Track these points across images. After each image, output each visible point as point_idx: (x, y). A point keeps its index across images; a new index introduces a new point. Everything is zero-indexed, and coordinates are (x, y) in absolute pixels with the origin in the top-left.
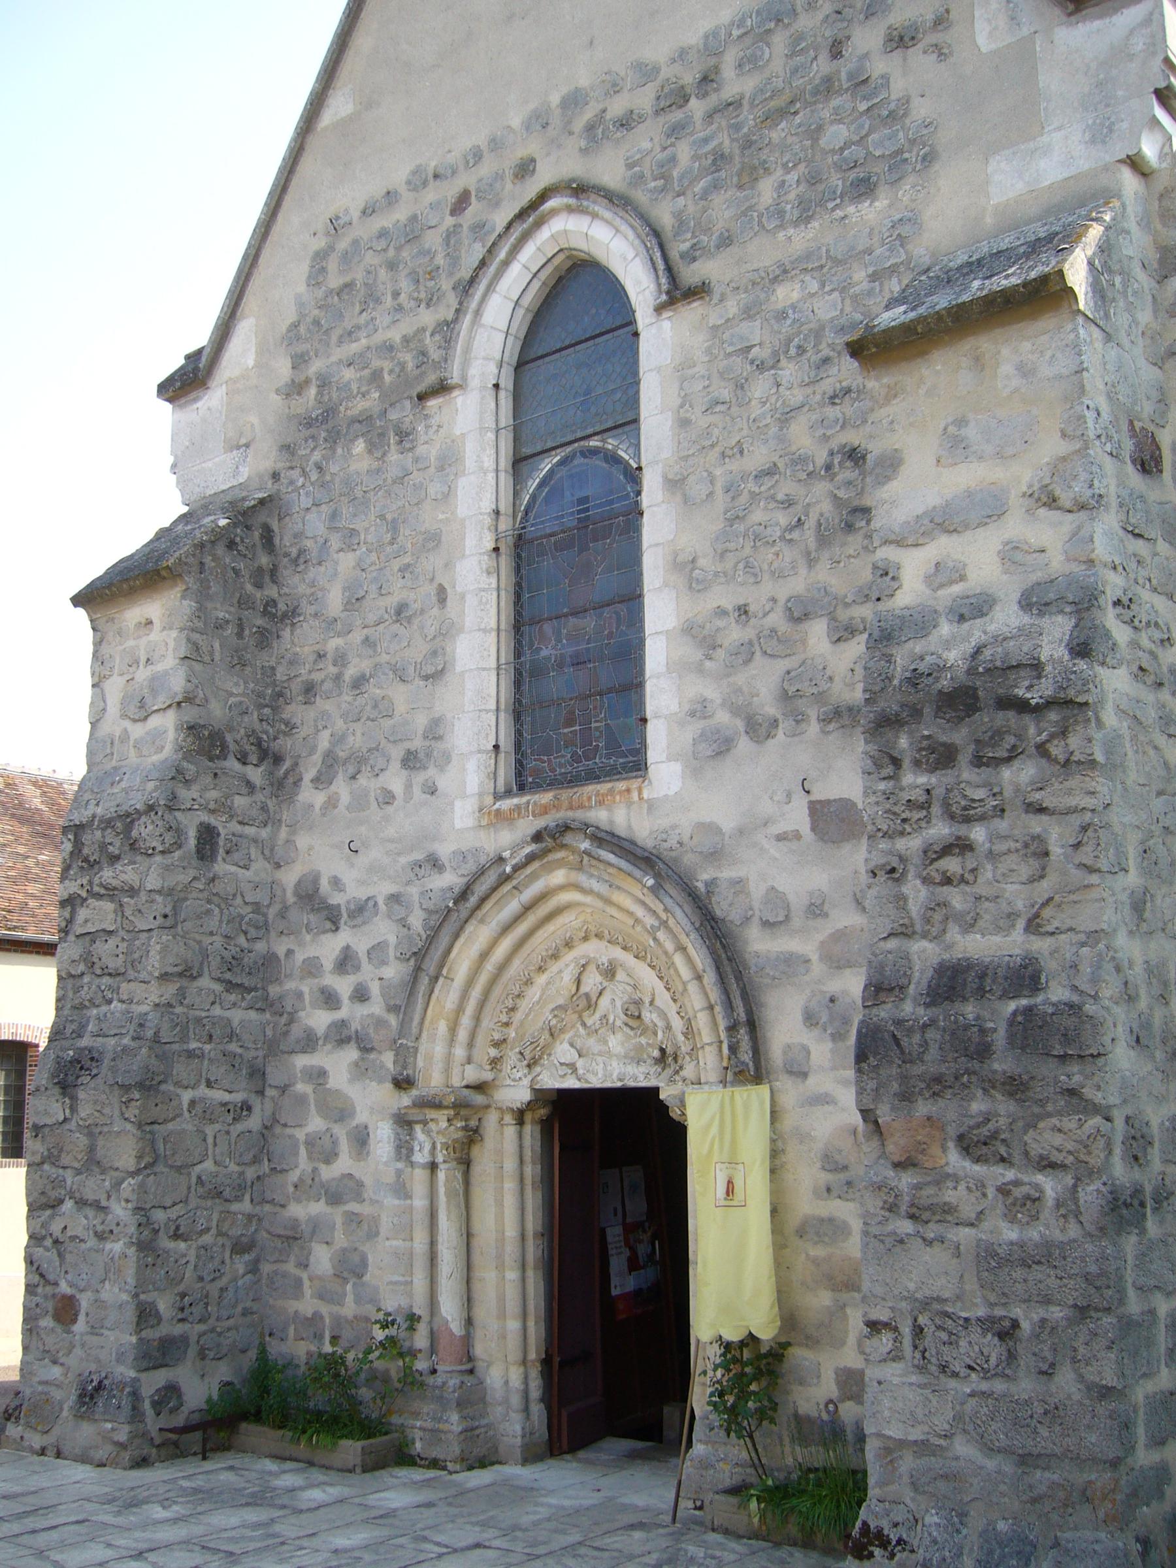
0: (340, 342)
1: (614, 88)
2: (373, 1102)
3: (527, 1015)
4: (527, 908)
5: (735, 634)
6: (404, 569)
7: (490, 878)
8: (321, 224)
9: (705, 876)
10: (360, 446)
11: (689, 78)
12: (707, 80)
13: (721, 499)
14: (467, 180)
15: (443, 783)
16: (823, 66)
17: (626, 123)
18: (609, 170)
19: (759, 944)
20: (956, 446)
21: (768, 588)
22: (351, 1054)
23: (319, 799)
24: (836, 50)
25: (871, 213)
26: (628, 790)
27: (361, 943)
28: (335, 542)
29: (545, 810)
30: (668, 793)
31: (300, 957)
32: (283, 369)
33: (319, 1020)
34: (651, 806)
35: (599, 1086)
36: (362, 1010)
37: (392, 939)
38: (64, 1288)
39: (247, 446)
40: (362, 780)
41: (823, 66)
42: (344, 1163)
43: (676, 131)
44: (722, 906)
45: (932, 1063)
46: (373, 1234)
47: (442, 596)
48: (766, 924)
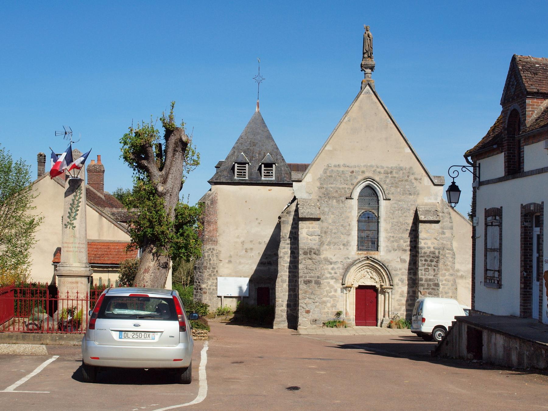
1: (377, 167)
2: (339, 286)
5: (392, 239)
6: (343, 220)
7: (358, 261)
8: (326, 165)
10: (335, 201)
11: (389, 171)
12: (391, 172)
14: (354, 169)
15: (349, 249)
16: (406, 178)
17: (380, 172)
18: (377, 178)
19: (393, 273)
20: (427, 232)
21: (396, 235)
22: (334, 280)
23: (328, 247)
24: (408, 176)
27: (336, 267)
28: (330, 213)
30: (381, 255)
31: (324, 267)
32: (318, 184)
33: (328, 275)
38: (307, 309)
40: (336, 246)
41: (406, 178)
42: (333, 293)
43: (387, 177)
44: (390, 268)
45: (426, 287)
46: (338, 301)
47: (349, 225)
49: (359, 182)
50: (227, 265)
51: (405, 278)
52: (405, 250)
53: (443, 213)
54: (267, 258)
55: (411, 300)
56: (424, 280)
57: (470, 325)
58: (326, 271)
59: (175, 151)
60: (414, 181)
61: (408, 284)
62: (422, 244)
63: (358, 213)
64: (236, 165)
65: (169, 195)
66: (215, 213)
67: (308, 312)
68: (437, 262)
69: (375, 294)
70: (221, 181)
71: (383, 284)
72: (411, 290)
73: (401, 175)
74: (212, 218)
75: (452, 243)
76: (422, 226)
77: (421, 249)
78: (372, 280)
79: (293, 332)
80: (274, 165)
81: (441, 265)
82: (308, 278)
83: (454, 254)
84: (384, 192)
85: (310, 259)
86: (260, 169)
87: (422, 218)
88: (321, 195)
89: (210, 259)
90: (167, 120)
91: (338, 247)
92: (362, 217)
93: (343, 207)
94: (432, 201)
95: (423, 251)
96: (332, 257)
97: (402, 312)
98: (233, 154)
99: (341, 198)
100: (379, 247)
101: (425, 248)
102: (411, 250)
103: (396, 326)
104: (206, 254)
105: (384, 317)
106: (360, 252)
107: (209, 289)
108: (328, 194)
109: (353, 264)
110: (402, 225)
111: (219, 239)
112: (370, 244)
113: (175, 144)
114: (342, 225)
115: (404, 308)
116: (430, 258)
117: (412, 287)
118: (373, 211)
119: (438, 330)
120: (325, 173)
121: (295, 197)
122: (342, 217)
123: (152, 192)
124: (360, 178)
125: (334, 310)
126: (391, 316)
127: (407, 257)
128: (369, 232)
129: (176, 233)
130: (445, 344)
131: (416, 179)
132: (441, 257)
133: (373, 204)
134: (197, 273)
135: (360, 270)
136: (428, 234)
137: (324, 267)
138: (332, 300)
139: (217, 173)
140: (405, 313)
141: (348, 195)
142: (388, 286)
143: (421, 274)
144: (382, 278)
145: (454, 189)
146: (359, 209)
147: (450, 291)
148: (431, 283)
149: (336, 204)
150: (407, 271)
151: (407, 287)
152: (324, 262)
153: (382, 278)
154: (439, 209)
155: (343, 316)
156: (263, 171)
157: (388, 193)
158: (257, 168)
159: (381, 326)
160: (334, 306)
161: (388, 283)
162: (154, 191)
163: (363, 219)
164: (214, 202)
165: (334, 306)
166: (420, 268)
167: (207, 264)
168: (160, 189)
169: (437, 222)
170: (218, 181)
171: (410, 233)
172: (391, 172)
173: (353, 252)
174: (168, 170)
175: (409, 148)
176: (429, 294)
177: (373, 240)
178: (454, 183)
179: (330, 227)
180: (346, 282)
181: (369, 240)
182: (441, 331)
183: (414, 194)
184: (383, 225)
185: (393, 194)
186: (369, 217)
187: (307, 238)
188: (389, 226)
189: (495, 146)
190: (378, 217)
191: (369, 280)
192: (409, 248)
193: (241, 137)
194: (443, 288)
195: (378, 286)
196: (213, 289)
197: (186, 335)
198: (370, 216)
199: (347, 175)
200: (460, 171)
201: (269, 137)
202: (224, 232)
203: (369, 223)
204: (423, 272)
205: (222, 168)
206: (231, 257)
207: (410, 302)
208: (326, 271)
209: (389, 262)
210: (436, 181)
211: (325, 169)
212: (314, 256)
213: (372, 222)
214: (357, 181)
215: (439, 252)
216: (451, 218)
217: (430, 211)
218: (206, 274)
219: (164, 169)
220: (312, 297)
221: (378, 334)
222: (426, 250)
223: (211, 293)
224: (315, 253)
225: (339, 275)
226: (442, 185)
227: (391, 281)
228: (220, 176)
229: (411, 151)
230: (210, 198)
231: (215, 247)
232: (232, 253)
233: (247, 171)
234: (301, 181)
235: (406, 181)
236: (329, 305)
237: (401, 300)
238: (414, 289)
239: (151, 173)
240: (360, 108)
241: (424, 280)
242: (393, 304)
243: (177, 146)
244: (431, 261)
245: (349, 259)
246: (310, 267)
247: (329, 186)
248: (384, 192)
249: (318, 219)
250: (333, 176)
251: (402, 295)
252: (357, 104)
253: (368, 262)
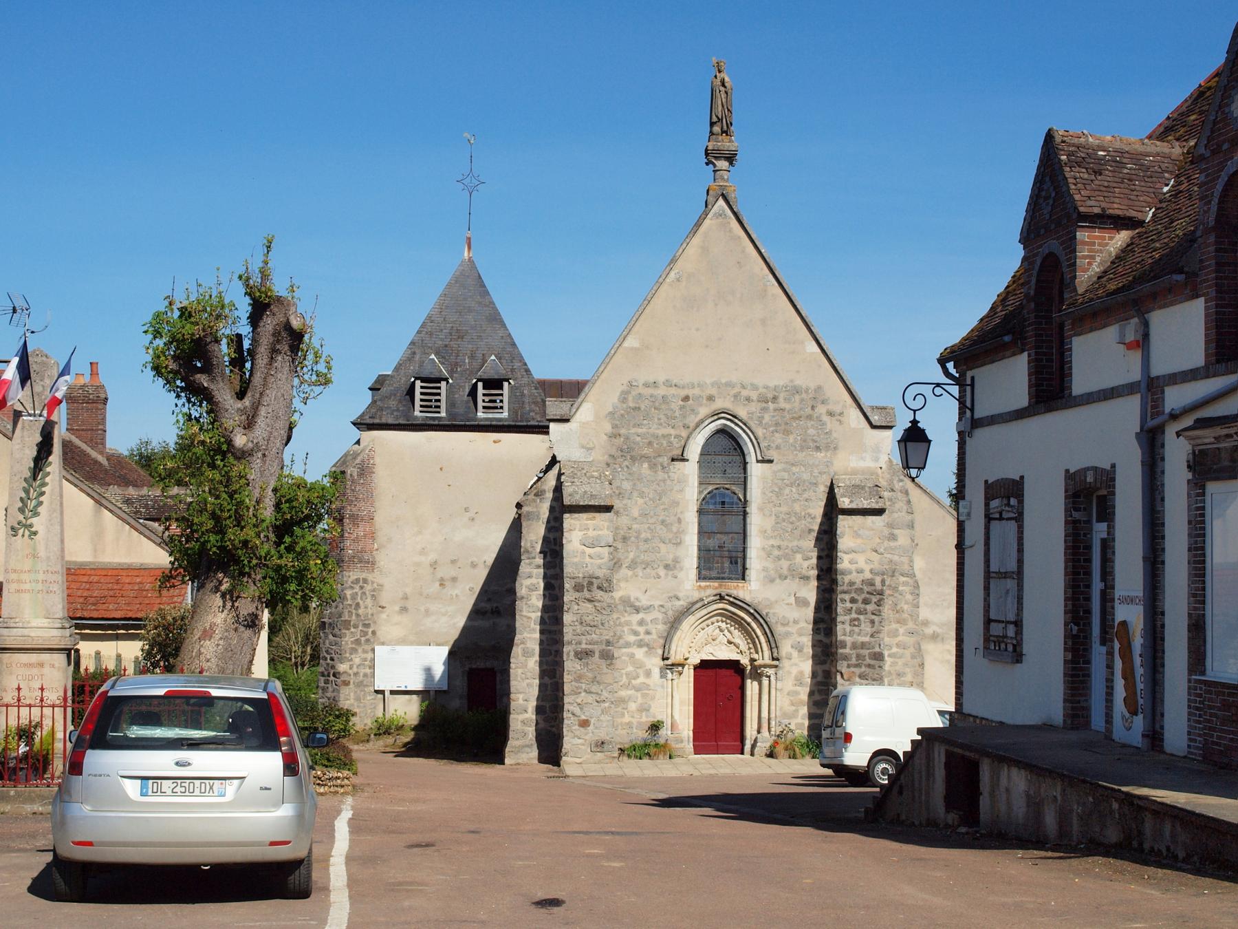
0: (634, 426)
1: (743, 387)
2: (655, 663)
5: (776, 553)
6: (664, 510)
8: (625, 382)
10: (646, 465)
11: (770, 396)
12: (775, 398)
13: (774, 517)
14: (690, 393)
15: (681, 575)
16: (808, 411)
17: (748, 399)
18: (742, 413)
19: (779, 630)
20: (856, 535)
21: (786, 543)
22: (645, 649)
23: (630, 573)
24: (813, 408)
25: (820, 455)
28: (635, 494)
30: (753, 589)
31: (623, 620)
32: (608, 427)
36: (648, 637)
38: (583, 717)
39: (589, 449)
40: (648, 570)
41: (808, 411)
42: (642, 679)
43: (764, 409)
44: (772, 620)
45: (854, 661)
46: (653, 698)
47: (679, 521)
48: (783, 625)
49: (702, 421)
50: (397, 618)
51: (807, 641)
52: (805, 578)
53: (893, 490)
54: (489, 600)
55: (820, 691)
56: (849, 645)
57: (951, 749)
58: (626, 629)
59: (274, 351)
60: (825, 418)
61: (814, 656)
62: (845, 562)
63: (700, 492)
64: (418, 384)
65: (260, 455)
66: (370, 497)
67: (584, 724)
68: (879, 603)
69: (739, 679)
70: (384, 421)
71: (756, 656)
72: (820, 669)
73: (797, 404)
74: (362, 508)
75: (912, 561)
76: (845, 523)
77: (843, 574)
79: (550, 770)
80: (506, 384)
81: (886, 610)
82: (584, 646)
83: (917, 586)
84: (757, 444)
85: (590, 601)
86: (473, 393)
87: (844, 502)
88: (613, 451)
89: (358, 605)
90: (256, 279)
91: (653, 573)
92: (707, 503)
93: (664, 481)
94: (867, 463)
95: (847, 579)
96: (639, 595)
97: (799, 720)
98: (410, 358)
99: (660, 460)
100: (747, 572)
101: (850, 573)
102: (819, 578)
103: (787, 753)
104: (348, 593)
105: (759, 732)
106: (703, 584)
107: (356, 674)
108: (630, 449)
110: (799, 519)
111: (377, 559)
112: (727, 564)
113: (273, 335)
114: (663, 522)
115: (804, 710)
116: (863, 596)
117: (823, 663)
118: (734, 488)
119: (879, 761)
120: (623, 399)
121: (554, 457)
122: (663, 504)
123: (220, 448)
124: (704, 411)
125: (644, 719)
126: (776, 730)
127: (810, 593)
128: (724, 538)
129: (278, 544)
130: (896, 789)
131: (831, 414)
132: (888, 592)
133: (734, 472)
134: (326, 637)
136: (859, 541)
137: (623, 620)
138: (639, 695)
139: (374, 402)
140: (806, 723)
141: (678, 452)
142: (767, 661)
143: (843, 631)
144: (754, 643)
145: (915, 437)
146: (701, 484)
147: (908, 670)
148: (866, 652)
149: (648, 472)
150: (811, 626)
151: (810, 662)
152: (621, 607)
153: (754, 643)
154: (883, 483)
155: (665, 732)
156: (480, 398)
157: (768, 447)
158: (467, 390)
159: (752, 754)
160: (644, 709)
162: (224, 447)
163: (711, 507)
164: (365, 470)
165: (644, 709)
166: (839, 619)
167: (350, 616)
168: (240, 440)
169: (879, 512)
170: (377, 421)
171: (817, 539)
172: (775, 398)
173: (688, 583)
174: (258, 395)
175: (814, 343)
176: (860, 677)
177: (734, 554)
178: (915, 422)
179: (635, 526)
180: (672, 652)
181: (724, 556)
182: (887, 761)
183: (827, 448)
184: (757, 522)
185: (778, 447)
186: (723, 503)
187: (583, 552)
188: (769, 523)
189: (1007, 338)
190: (746, 501)
192: (815, 572)
193: (430, 319)
194: (894, 664)
195: (745, 661)
196: (365, 675)
197: (300, 786)
198: (727, 500)
199: (673, 406)
200: (929, 394)
201: (495, 318)
202: (390, 540)
203: (724, 514)
204: (848, 628)
205: (383, 390)
206: (406, 598)
207: (817, 697)
208: (626, 629)
209: (770, 606)
210: (875, 419)
211: (623, 392)
212: (599, 594)
213: (730, 513)
214: (697, 420)
215: (883, 582)
216: (909, 502)
217: (863, 488)
218: (348, 640)
219: (249, 394)
220: (594, 688)
221: (745, 771)
222: (857, 578)
223: (360, 685)
224: (599, 588)
225: (655, 638)
226: (890, 427)
227: (775, 650)
228: (381, 409)
229: (819, 350)
230: (358, 461)
231: (370, 577)
232: (408, 590)
233: (443, 397)
234: (567, 421)
235: (809, 417)
236: (633, 706)
237: (797, 693)
238: (826, 667)
239: (217, 404)
240: (705, 250)
241: (849, 645)
242: (778, 702)
243: (278, 341)
244: (866, 602)
245: (678, 599)
246: (588, 619)
247: (633, 431)
248: (757, 444)
249: (608, 509)
250: (643, 407)
251: (799, 681)
252: (697, 240)
253: (721, 606)
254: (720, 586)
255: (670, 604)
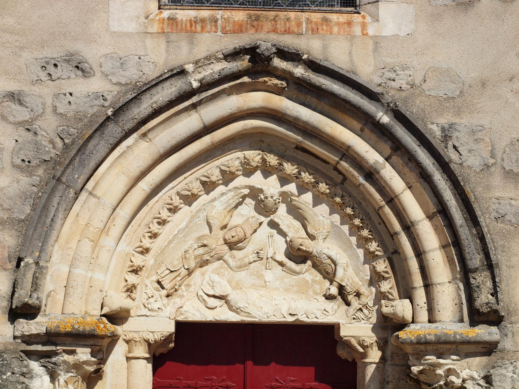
3: (170, 242)
4: (208, 129)
9: (444, 120)
26: (349, 24)
29: (239, 29)
34: (377, 42)
35: (265, 319)
37: (9, 144)
48: (508, 174)
71: (402, 308)
78: (307, 273)
106: (185, 14)
109: (120, 119)
135: (190, 181)
144: (394, 256)
153: (394, 256)
161: (448, 294)
191: (273, 275)
195: (357, 329)
227: (482, 279)
245: (81, 68)
253: (257, 99)
254: (255, 23)
255: (46, 91)
